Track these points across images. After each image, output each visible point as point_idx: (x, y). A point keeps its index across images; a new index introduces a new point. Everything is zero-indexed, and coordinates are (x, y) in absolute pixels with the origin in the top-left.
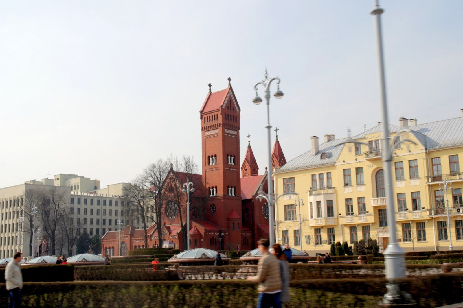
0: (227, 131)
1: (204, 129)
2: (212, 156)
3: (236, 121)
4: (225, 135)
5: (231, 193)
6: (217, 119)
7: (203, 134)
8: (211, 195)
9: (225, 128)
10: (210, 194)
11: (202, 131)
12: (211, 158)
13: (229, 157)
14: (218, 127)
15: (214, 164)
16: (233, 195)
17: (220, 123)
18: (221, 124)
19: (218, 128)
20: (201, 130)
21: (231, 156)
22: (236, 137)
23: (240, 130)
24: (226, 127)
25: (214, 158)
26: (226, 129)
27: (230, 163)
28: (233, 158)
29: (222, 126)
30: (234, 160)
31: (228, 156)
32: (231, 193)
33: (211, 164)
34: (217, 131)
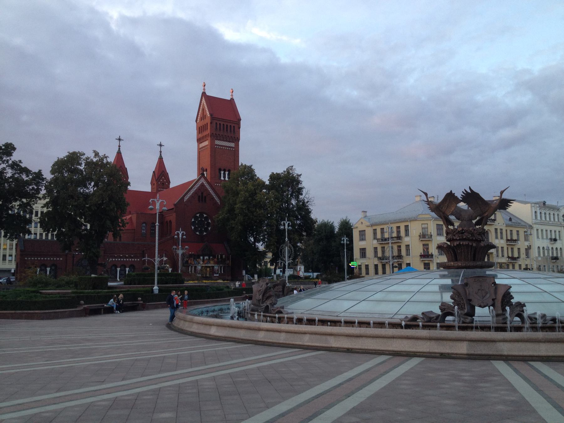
0: (217, 142)
1: (200, 140)
4: (216, 147)
6: (207, 129)
7: (198, 146)
9: (216, 139)
11: (198, 143)
13: (222, 172)
14: (208, 138)
18: (209, 134)
19: (208, 139)
20: (197, 142)
21: (225, 171)
22: (234, 149)
24: (215, 138)
26: (217, 139)
27: (222, 178)
28: (227, 173)
29: (210, 137)
30: (229, 174)
31: (220, 170)
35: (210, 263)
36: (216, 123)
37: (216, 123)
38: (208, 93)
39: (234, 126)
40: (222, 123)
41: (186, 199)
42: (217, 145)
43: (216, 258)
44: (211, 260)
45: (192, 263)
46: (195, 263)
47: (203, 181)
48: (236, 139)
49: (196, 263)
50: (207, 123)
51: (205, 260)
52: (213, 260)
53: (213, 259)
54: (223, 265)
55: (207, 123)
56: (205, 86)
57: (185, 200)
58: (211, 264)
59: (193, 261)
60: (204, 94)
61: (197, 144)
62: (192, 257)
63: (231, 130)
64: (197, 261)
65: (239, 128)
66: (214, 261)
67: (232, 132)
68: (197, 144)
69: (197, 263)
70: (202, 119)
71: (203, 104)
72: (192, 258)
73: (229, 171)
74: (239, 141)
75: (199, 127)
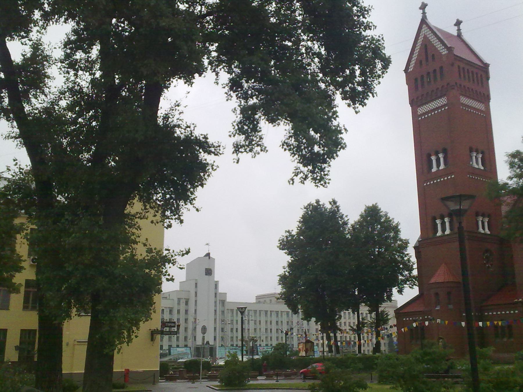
0: (464, 100)
2: (437, 154)
3: (482, 83)
5: (483, 228)
8: (439, 233)
9: (463, 95)
10: (437, 231)
11: (411, 106)
12: (433, 158)
13: (474, 154)
15: (442, 167)
16: (487, 231)
17: (448, 84)
19: (445, 95)
21: (477, 152)
23: (490, 103)
25: (441, 156)
31: (471, 150)
32: (483, 228)
33: (434, 169)
34: (443, 101)
36: (459, 66)
37: (459, 66)
38: (432, 21)
39: (481, 76)
40: (467, 67)
42: (463, 104)
48: (486, 98)
50: (441, 68)
55: (441, 68)
56: (423, 7)
60: (424, 22)
61: (409, 109)
63: (478, 81)
65: (488, 78)
67: (480, 84)
68: (410, 108)
70: (424, 62)
71: (425, 37)
73: (482, 153)
74: (489, 102)
75: (416, 80)
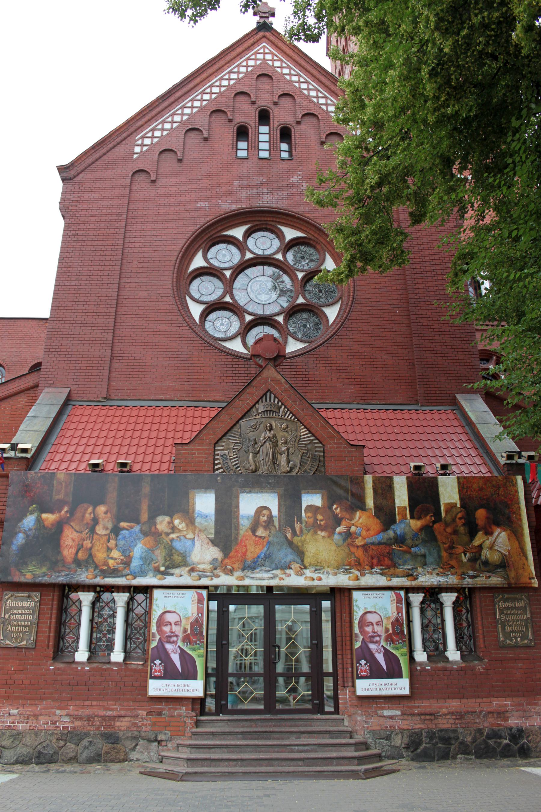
35: (301, 554)
41: (147, 141)
43: (362, 507)
44: (316, 527)
45: (100, 555)
46: (127, 563)
47: (269, 57)
49: (147, 560)
51: (245, 524)
52: (330, 529)
53: (338, 522)
54: (452, 580)
57: (137, 149)
58: (319, 567)
59: (116, 531)
62: (101, 502)
64: (157, 535)
66: (348, 535)
69: (159, 555)
72: (102, 509)
